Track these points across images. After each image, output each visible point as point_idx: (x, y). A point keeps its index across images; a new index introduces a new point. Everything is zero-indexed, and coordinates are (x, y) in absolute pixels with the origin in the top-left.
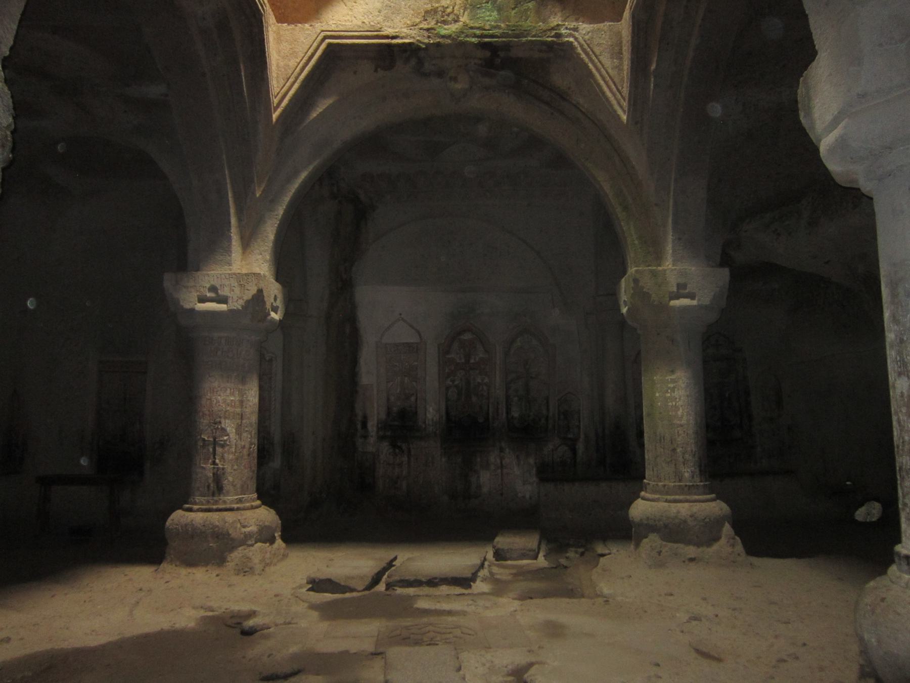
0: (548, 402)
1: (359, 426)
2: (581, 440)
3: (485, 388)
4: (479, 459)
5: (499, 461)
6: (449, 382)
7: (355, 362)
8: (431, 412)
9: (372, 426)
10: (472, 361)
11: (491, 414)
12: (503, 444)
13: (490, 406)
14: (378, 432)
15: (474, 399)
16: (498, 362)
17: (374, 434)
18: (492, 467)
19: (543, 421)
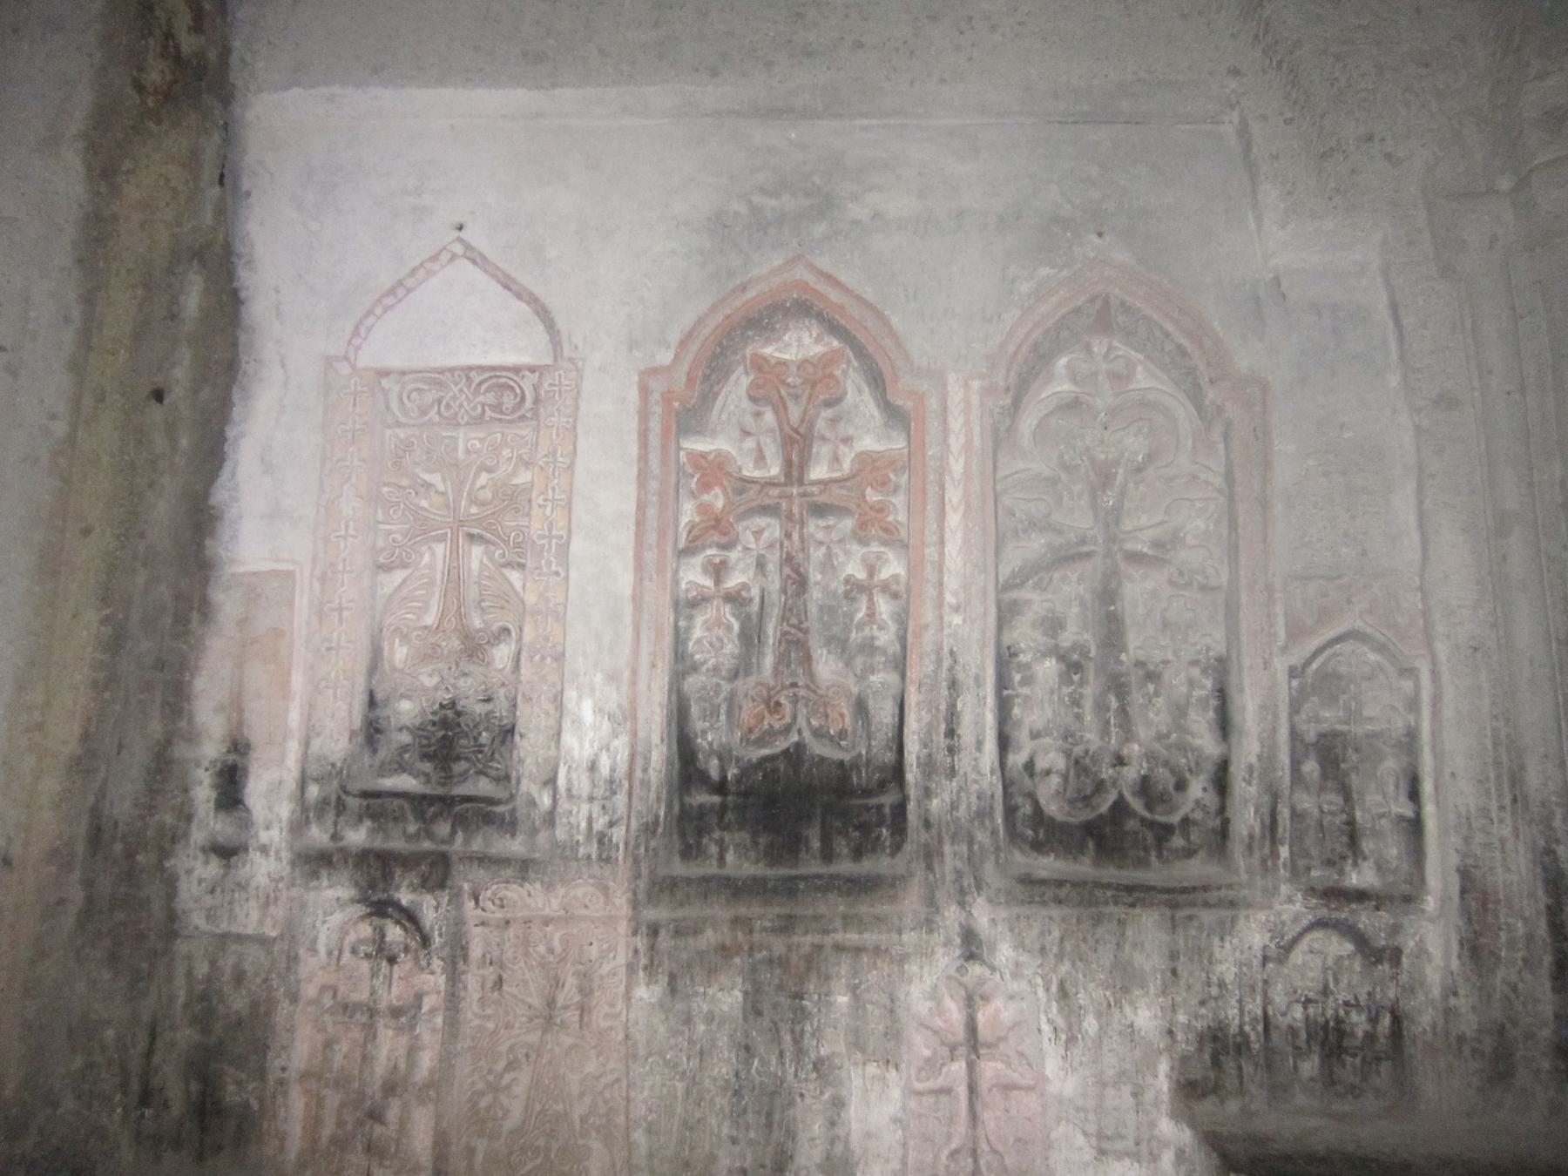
0: (1222, 694)
1: (204, 793)
2: (1431, 903)
3: (884, 607)
4: (842, 999)
5: (955, 1012)
6: (694, 575)
7: (211, 454)
8: (591, 734)
9: (271, 794)
10: (818, 472)
11: (913, 749)
12: (983, 915)
13: (912, 698)
14: (297, 827)
15: (827, 667)
16: (957, 466)
17: (274, 836)
18: (921, 1045)
19: (1198, 789)
